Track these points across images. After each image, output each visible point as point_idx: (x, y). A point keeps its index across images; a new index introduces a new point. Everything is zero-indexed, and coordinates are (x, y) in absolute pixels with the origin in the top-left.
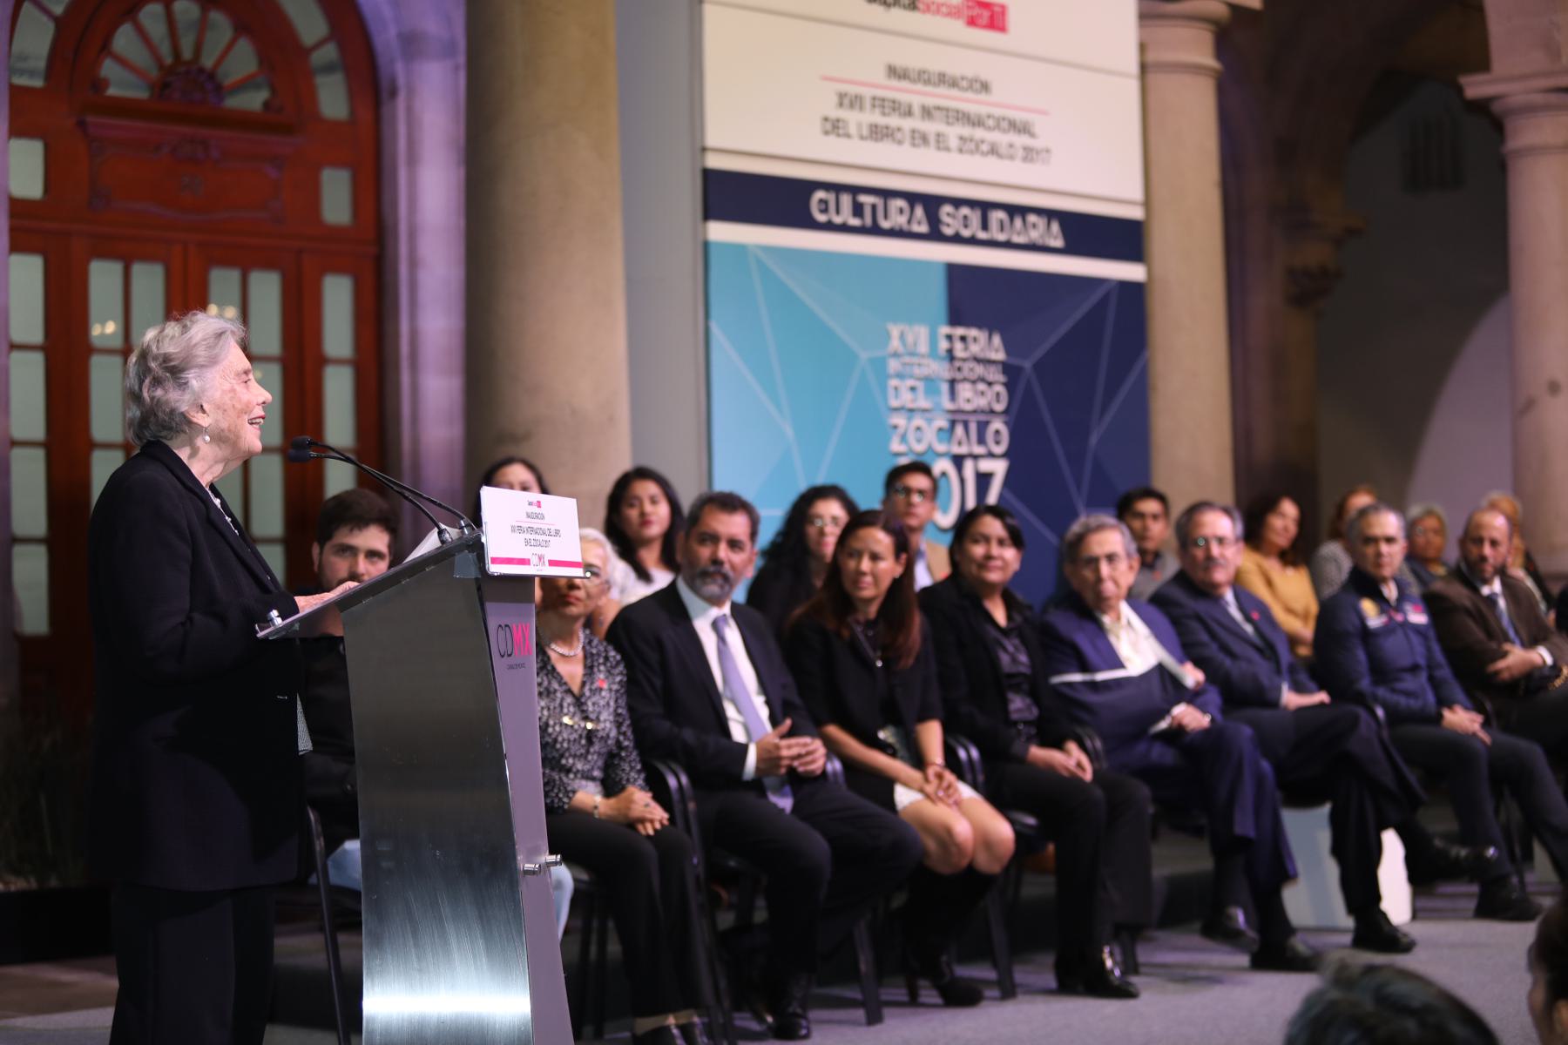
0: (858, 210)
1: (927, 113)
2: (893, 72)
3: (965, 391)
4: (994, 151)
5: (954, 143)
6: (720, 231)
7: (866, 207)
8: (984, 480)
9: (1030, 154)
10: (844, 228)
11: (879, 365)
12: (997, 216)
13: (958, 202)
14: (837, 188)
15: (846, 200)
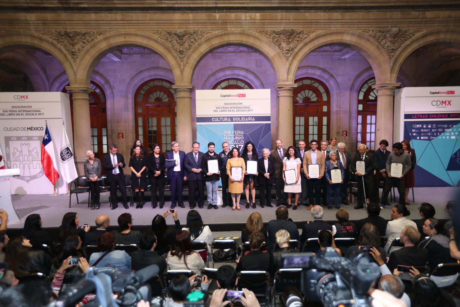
0: (219, 119)
1: (231, 108)
2: (225, 104)
3: (236, 138)
7: (221, 119)
9: (249, 111)
10: (217, 121)
12: (242, 118)
13: (236, 117)
14: (216, 117)
15: (217, 119)
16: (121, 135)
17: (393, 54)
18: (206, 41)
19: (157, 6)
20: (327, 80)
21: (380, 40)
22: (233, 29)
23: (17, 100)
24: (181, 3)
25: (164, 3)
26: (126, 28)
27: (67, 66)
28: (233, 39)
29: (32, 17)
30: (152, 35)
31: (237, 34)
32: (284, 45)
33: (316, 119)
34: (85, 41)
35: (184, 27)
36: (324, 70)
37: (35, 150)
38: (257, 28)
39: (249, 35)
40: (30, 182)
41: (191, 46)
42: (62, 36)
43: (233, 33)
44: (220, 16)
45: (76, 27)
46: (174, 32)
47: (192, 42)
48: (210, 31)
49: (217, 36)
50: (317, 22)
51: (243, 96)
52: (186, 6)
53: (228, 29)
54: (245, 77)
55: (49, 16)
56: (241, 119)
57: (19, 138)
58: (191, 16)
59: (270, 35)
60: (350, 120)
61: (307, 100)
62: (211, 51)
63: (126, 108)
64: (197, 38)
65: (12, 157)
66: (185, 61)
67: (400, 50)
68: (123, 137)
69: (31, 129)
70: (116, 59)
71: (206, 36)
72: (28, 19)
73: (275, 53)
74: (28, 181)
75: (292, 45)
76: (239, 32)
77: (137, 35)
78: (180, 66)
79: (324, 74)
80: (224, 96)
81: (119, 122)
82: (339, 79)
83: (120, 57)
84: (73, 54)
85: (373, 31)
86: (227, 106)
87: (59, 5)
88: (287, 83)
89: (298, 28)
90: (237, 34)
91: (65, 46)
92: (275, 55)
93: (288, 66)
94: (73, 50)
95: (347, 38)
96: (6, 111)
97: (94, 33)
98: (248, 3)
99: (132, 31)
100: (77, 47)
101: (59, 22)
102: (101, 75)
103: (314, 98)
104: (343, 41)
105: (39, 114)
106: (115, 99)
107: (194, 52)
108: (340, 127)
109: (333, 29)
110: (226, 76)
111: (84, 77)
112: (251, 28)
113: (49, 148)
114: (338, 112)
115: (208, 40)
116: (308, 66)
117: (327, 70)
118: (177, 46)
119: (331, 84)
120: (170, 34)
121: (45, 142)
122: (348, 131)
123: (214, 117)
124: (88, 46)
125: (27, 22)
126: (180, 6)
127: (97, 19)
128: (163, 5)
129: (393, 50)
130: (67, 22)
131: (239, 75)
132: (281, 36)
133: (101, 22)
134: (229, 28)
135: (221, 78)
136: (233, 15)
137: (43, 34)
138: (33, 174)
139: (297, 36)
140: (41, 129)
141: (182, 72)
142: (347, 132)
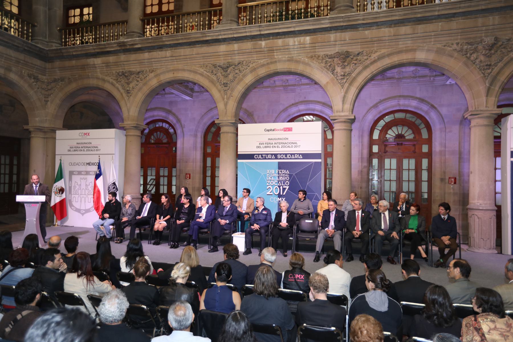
0: (262, 156)
1: (275, 143)
2: (269, 139)
3: (281, 178)
4: (288, 147)
5: (280, 147)
6: (239, 161)
7: (264, 156)
8: (284, 189)
9: (295, 147)
10: (260, 159)
11: (265, 175)
12: (288, 156)
13: (281, 154)
14: (259, 154)
15: (260, 156)
16: (188, 176)
17: (489, 71)
18: (251, 72)
19: (202, 39)
20: (427, 113)
21: (468, 55)
22: (280, 57)
23: (81, 137)
24: (224, 35)
25: (209, 36)
26: (174, 64)
27: (122, 104)
28: (280, 67)
29: (98, 61)
30: (198, 68)
31: (285, 61)
32: (338, 69)
33: (413, 162)
34: (139, 79)
35: (230, 58)
36: (422, 100)
37: (91, 184)
38: (308, 53)
39: (297, 62)
40: (85, 215)
41: (236, 77)
42: (120, 76)
43: (280, 61)
44: (266, 44)
45: (132, 67)
46: (218, 64)
47: (237, 73)
48: (256, 61)
49: (263, 65)
50: (380, 40)
51: (290, 129)
52: (230, 36)
53: (275, 57)
54: (321, 112)
55: (111, 59)
56: (286, 156)
57: (80, 173)
58: (236, 46)
59: (323, 59)
60: (459, 162)
61: (400, 136)
62: (259, 83)
63: (195, 148)
64: (241, 69)
65: (73, 190)
66: (228, 95)
67: (500, 65)
68: (190, 178)
69: (89, 164)
70: (188, 98)
71: (251, 66)
72: (96, 63)
73: (328, 80)
74: (83, 214)
75: (348, 70)
76: (286, 59)
77: (184, 70)
78: (224, 99)
79: (422, 104)
80: (268, 130)
81: (187, 162)
82: (444, 111)
83: (191, 96)
84: (128, 92)
85: (458, 44)
86: (271, 142)
87: (119, 48)
88: (342, 114)
89: (355, 49)
90: (285, 61)
91: (123, 86)
92: (328, 83)
93: (343, 94)
94: (128, 89)
95: (421, 56)
96: (72, 148)
97: (146, 71)
98: (294, 27)
99: (180, 66)
100: (131, 85)
101: (119, 64)
102: (174, 115)
103: (409, 135)
104: (416, 60)
105: (97, 150)
106: (185, 138)
107: (238, 84)
108: (445, 173)
109: (401, 45)
110: (299, 111)
111: (136, 114)
112: (300, 53)
113: (100, 182)
114: (442, 153)
115: (254, 70)
116: (400, 96)
117: (426, 99)
118: (222, 78)
119: (432, 117)
120: (215, 66)
121: (97, 176)
122: (457, 178)
123: (257, 154)
124: (140, 84)
125: (94, 66)
126: (224, 37)
127: (150, 58)
128: (208, 38)
129: (490, 65)
130: (125, 63)
131: (314, 110)
132: (336, 59)
133: (153, 60)
134: (277, 55)
135: (294, 114)
136: (280, 42)
137: (106, 75)
138: (87, 208)
139: (355, 58)
140: (93, 164)
141: (226, 105)
142: (455, 179)
